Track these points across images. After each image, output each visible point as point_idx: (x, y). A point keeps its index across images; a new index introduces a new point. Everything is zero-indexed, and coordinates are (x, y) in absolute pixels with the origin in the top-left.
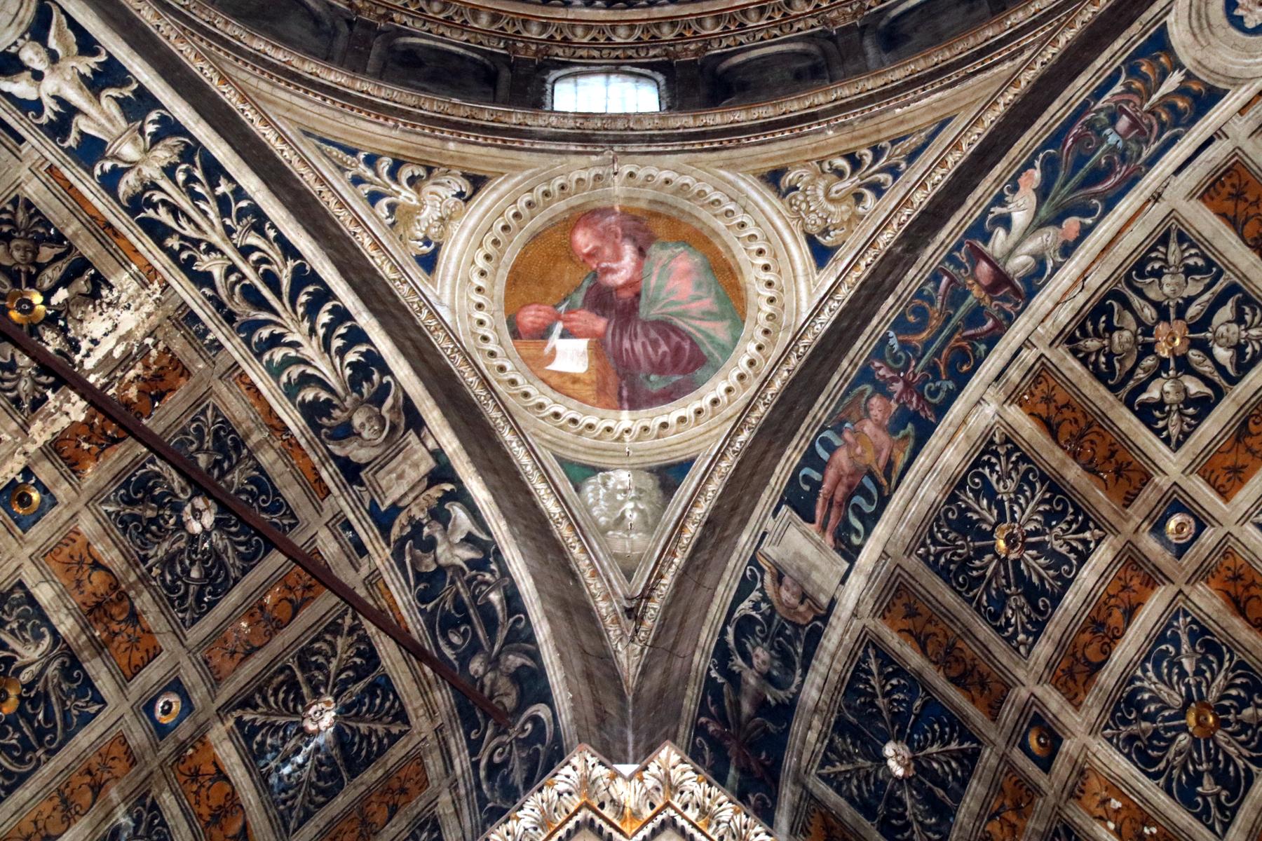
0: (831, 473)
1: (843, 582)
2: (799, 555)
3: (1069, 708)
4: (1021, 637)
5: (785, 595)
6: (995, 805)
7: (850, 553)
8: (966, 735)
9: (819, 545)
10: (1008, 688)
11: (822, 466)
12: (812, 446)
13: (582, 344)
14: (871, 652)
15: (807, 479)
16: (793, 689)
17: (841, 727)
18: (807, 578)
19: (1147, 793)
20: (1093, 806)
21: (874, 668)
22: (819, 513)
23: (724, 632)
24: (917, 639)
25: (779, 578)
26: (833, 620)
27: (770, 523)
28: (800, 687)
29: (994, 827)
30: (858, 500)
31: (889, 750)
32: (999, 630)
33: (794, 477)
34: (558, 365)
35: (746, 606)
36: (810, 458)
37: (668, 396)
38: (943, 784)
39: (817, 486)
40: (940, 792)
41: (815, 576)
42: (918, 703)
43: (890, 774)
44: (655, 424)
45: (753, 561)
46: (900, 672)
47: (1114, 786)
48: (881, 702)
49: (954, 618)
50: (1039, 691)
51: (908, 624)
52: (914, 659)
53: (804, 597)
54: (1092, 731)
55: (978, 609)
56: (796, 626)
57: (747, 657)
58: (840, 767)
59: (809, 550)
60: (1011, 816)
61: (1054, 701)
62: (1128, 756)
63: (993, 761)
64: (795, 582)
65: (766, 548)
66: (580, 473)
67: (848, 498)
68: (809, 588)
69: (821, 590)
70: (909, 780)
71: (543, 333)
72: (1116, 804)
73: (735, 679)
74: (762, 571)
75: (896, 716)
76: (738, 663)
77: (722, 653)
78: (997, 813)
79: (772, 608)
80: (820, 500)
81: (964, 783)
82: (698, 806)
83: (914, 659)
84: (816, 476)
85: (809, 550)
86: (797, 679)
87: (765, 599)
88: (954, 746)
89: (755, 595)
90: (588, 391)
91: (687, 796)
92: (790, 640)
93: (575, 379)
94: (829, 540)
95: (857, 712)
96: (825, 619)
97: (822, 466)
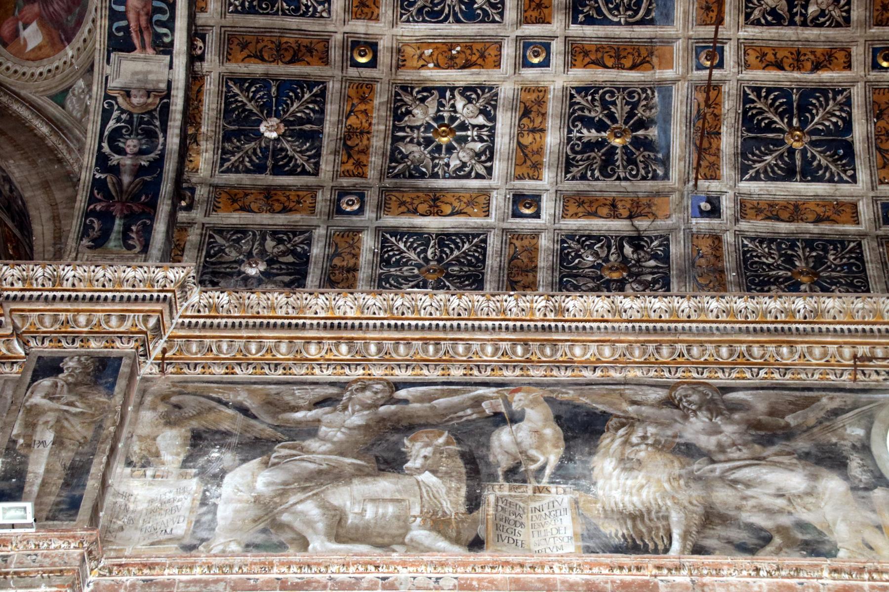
0: (132, 16)
1: (171, 67)
2: (135, 73)
3: (372, 23)
4: (320, 8)
5: (135, 101)
6: (347, 108)
7: (167, 49)
8: (311, 85)
9: (145, 60)
10: (327, 41)
11: (123, 16)
12: (111, 9)
13: (34, 26)
14: (231, 84)
15: (119, 29)
16: (160, 147)
17: (227, 137)
18: (146, 81)
19: (444, 32)
20: (415, 63)
21: (236, 91)
22: (137, 42)
23: (100, 147)
24: (256, 57)
25: (127, 94)
26: (173, 92)
27: (108, 70)
28: (164, 144)
29: (353, 120)
30: (157, 17)
31: (262, 128)
32: (304, 15)
33: (111, 35)
34: (31, 46)
35: (112, 124)
36: (114, 16)
37: (79, 23)
38: (309, 121)
39: (126, 29)
40: (307, 127)
41: (151, 77)
42: (274, 89)
43: (270, 140)
44: (80, 44)
45: (107, 97)
46: (254, 81)
47: (421, 44)
48: (250, 106)
49: (270, 30)
50: (347, 29)
51: (246, 52)
52: (258, 68)
53: (148, 93)
54: (394, 24)
55: (284, 14)
56: (150, 113)
57: (121, 152)
58: (233, 159)
59: (139, 66)
60: (362, 107)
61: (360, 27)
62: (424, 21)
63: (337, 86)
64: (139, 89)
65: (111, 84)
66: (60, 98)
67: (150, 21)
68: (150, 86)
69: (159, 81)
70: (283, 135)
71: (16, 34)
72: (428, 52)
73: (116, 170)
74: (115, 98)
75: (261, 108)
76: (115, 158)
77: (102, 160)
78: (351, 111)
79: (131, 114)
80: (134, 35)
81: (322, 111)
82: (19, 279)
83: (258, 68)
84: (123, 23)
85: (139, 66)
86: (161, 140)
87: (123, 111)
88: (307, 96)
89: (116, 114)
90: (47, 50)
91: (10, 279)
92: (149, 123)
93: (39, 48)
94: (150, 51)
95: (237, 121)
96: (168, 96)
97: (123, 16)
